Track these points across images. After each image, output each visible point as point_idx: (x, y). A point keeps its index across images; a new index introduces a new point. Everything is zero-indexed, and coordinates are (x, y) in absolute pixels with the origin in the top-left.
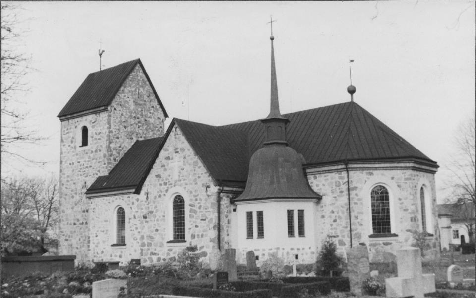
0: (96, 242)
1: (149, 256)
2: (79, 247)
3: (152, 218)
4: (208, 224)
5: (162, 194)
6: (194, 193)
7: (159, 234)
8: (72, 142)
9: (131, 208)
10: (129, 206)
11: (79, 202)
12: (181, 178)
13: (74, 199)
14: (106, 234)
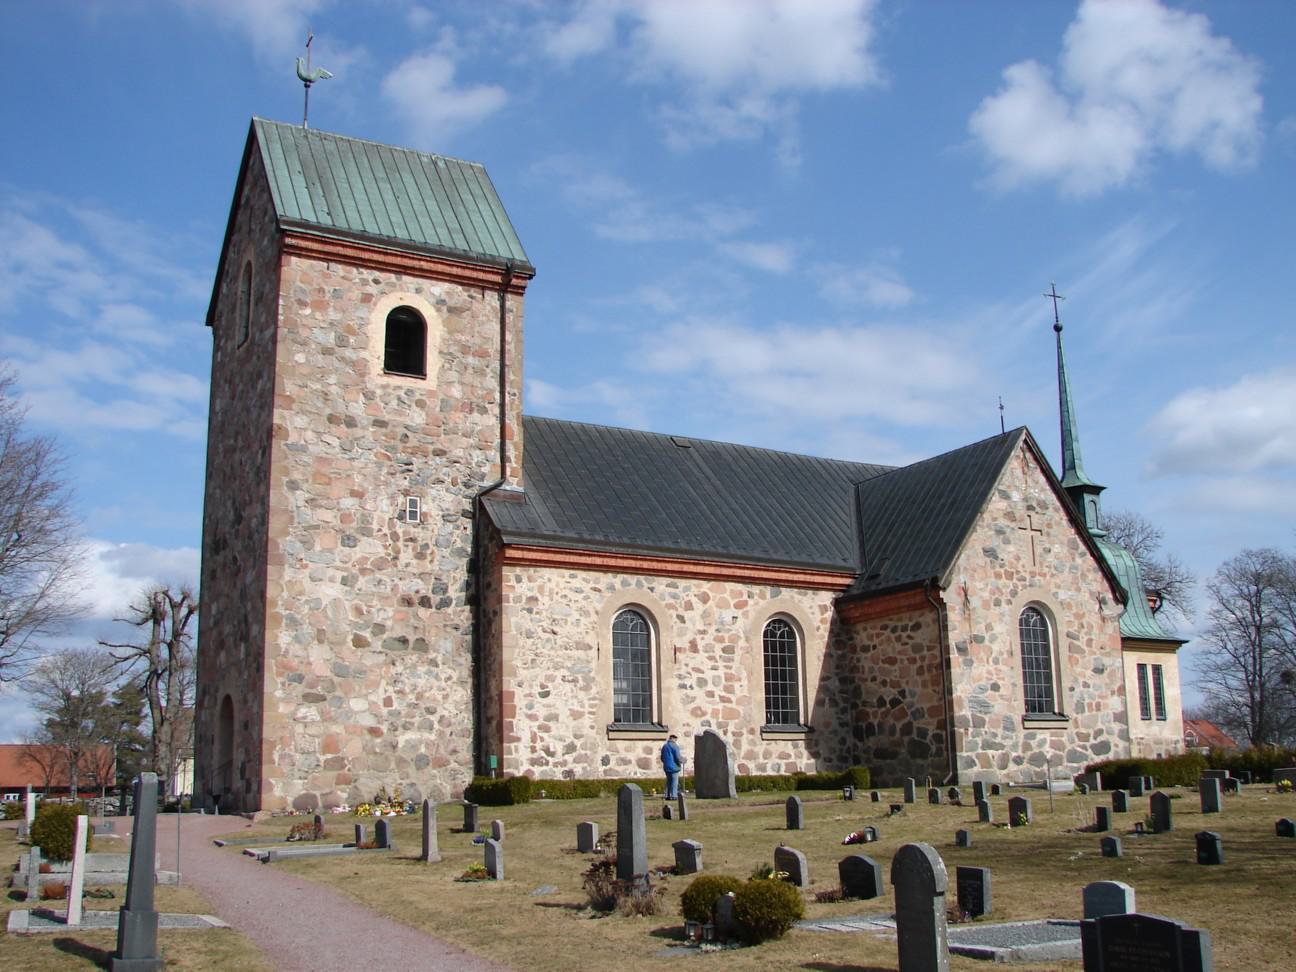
0: (541, 711)
1: (980, 751)
2: (384, 728)
3: (982, 655)
4: (1108, 681)
5: (1003, 599)
6: (1074, 610)
7: (1001, 696)
8: (342, 342)
9: (681, 619)
10: (674, 613)
11: (380, 565)
12: (1046, 570)
13: (357, 553)
14: (586, 688)
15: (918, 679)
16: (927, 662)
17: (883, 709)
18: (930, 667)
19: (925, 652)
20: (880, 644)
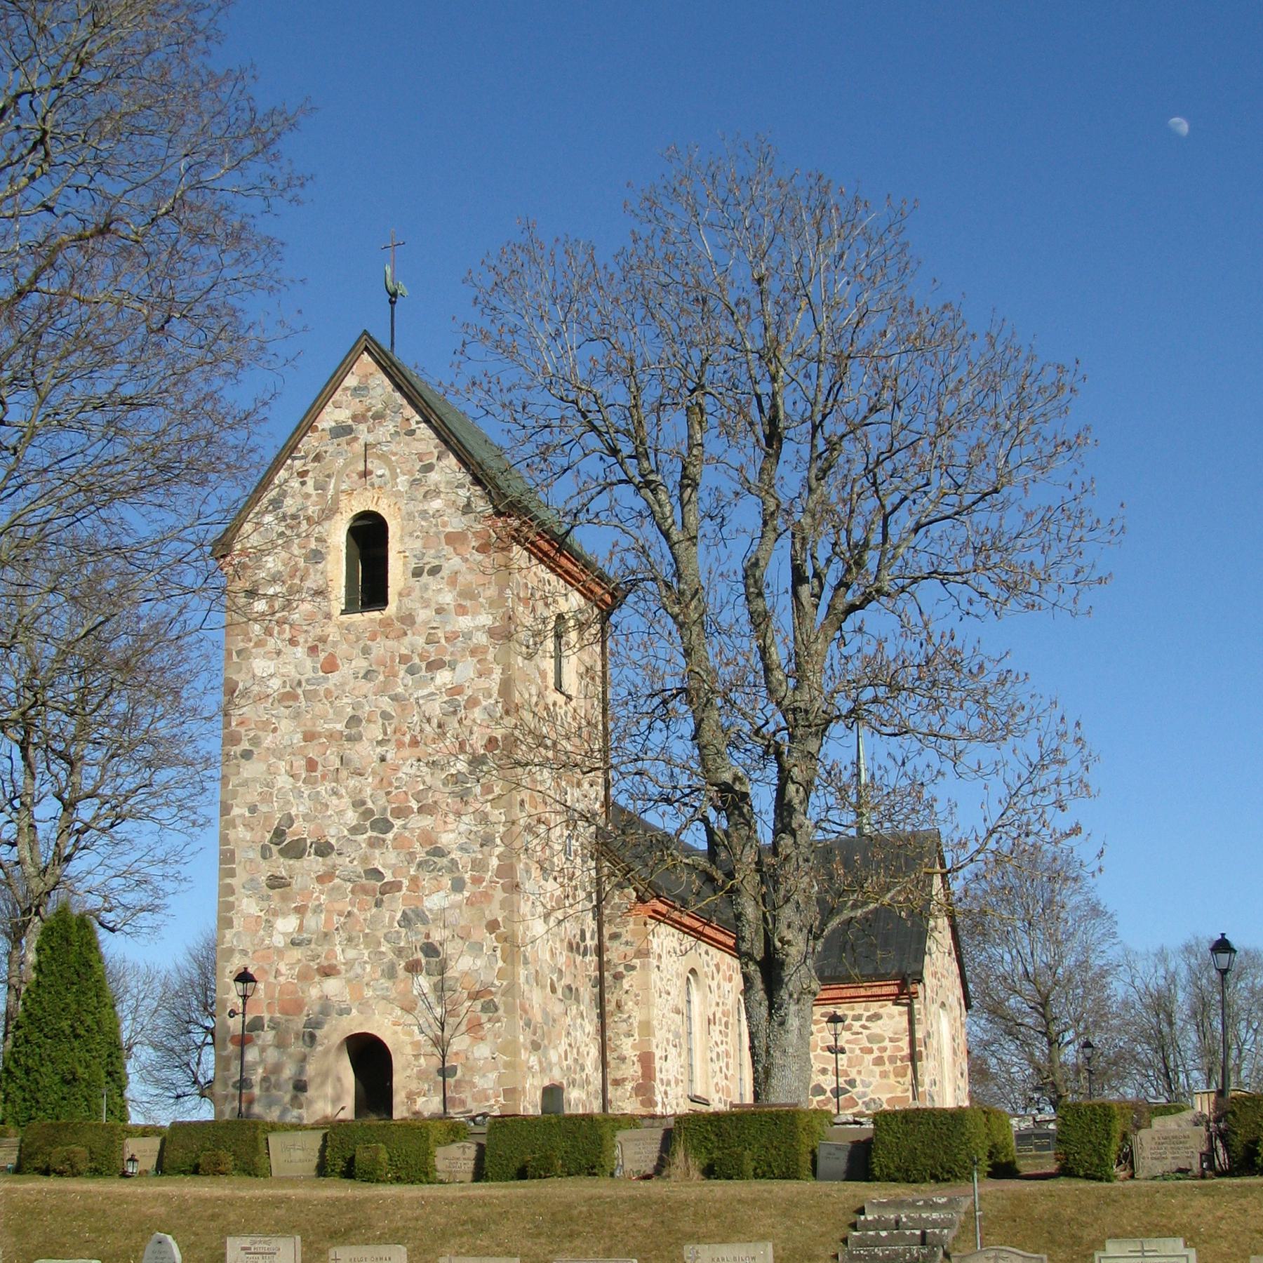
15: (877, 1069)
16: (888, 1053)
17: (822, 1097)
18: (892, 1059)
19: (887, 1043)
20: (819, 1032)
